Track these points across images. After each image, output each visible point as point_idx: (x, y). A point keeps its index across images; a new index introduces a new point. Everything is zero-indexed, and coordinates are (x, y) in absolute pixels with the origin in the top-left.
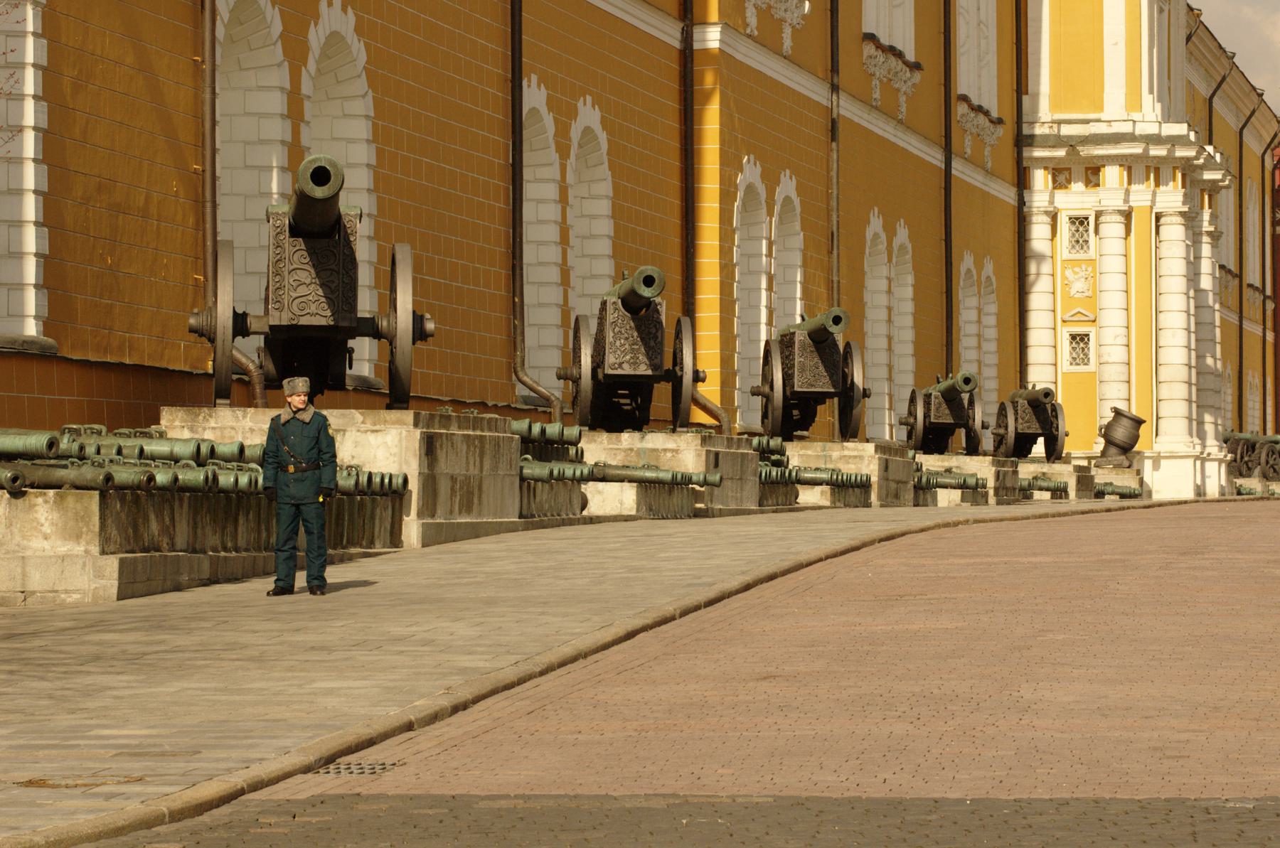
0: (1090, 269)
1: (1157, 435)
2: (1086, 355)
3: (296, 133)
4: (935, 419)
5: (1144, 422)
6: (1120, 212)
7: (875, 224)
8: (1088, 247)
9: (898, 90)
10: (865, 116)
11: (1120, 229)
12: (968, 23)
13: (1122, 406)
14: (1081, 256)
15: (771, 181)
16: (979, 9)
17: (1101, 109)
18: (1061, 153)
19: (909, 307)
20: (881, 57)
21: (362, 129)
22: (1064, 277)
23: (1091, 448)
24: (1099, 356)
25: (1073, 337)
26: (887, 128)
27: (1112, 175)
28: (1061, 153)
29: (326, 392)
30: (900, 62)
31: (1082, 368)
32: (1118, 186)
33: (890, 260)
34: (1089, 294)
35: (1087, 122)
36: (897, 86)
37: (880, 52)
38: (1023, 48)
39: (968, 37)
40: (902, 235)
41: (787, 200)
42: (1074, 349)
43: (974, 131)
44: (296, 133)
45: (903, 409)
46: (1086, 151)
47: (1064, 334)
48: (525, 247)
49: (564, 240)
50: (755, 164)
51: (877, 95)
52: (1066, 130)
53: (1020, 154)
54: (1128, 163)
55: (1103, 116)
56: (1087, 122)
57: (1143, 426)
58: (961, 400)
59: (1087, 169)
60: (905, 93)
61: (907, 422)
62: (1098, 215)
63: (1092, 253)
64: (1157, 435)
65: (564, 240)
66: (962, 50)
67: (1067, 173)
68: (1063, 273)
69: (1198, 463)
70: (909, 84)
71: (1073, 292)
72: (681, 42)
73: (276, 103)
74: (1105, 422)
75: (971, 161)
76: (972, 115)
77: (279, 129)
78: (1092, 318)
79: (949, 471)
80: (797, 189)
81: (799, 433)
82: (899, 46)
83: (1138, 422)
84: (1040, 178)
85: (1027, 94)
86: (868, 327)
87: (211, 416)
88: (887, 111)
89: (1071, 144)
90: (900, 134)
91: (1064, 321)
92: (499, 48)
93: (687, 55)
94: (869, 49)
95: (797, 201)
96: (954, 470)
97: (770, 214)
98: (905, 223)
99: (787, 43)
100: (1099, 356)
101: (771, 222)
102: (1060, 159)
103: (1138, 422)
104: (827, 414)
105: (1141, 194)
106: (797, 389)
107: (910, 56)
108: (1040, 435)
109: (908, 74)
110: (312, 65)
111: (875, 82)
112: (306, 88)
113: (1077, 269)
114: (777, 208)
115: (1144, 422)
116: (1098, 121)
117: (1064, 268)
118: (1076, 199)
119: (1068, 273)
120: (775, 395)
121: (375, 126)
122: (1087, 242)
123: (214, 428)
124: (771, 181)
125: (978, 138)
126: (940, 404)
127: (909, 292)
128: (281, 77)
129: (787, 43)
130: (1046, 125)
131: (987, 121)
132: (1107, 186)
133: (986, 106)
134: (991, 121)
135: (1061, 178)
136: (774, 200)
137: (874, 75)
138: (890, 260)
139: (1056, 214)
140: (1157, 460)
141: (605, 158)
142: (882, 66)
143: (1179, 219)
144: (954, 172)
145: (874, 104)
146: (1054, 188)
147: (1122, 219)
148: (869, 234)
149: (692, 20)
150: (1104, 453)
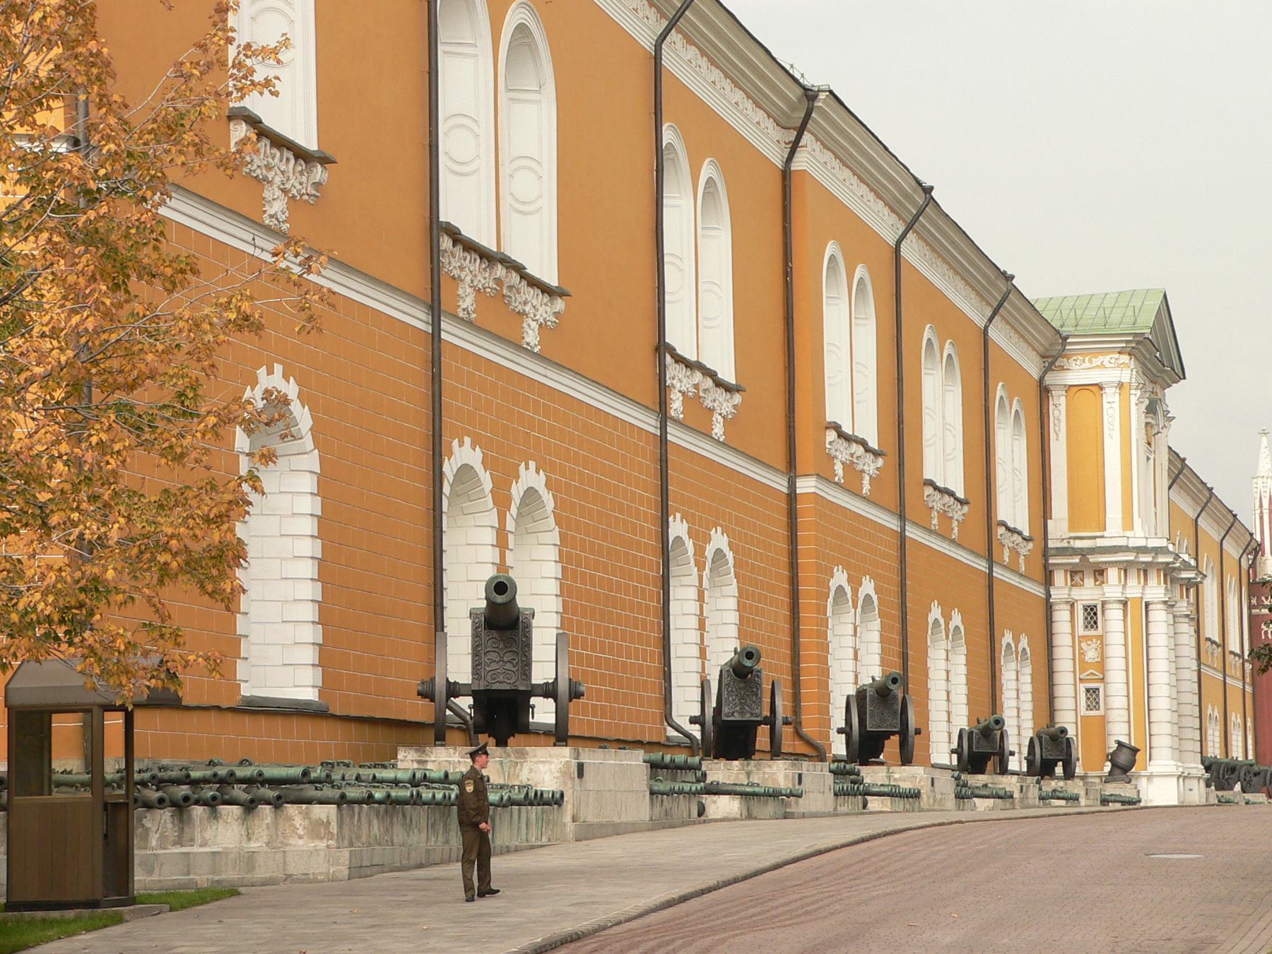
0: (1099, 642)
1: (1150, 759)
2: (1097, 703)
3: (502, 557)
4: (977, 748)
5: (1138, 750)
6: (1120, 602)
7: (936, 613)
8: (1097, 627)
9: (952, 518)
10: (927, 537)
11: (1119, 614)
12: (1005, 470)
13: (1125, 740)
14: (1092, 632)
15: (855, 583)
16: (1013, 460)
17: (1105, 530)
18: (1076, 560)
19: (963, 670)
20: (937, 495)
21: (553, 554)
22: (1081, 648)
23: (1103, 770)
24: (1105, 703)
25: (1088, 690)
26: (944, 545)
27: (1112, 574)
28: (1076, 560)
29: (516, 735)
30: (952, 499)
31: (1094, 713)
32: (1117, 583)
33: (947, 638)
34: (1099, 660)
35: (1095, 538)
36: (951, 515)
37: (937, 493)
38: (1048, 486)
39: (1005, 480)
40: (957, 619)
41: (868, 597)
42: (1088, 699)
43: (1011, 545)
44: (502, 557)
45: (955, 745)
46: (1093, 559)
47: (1082, 688)
48: (672, 632)
49: (702, 626)
50: (843, 572)
51: (935, 521)
52: (1078, 544)
53: (1046, 561)
54: (1125, 568)
55: (1106, 534)
56: (1095, 538)
57: (1138, 754)
58: (996, 735)
59: (1095, 571)
60: (957, 520)
61: (957, 751)
62: (1104, 603)
63: (1100, 631)
64: (1150, 759)
65: (702, 626)
66: (1001, 489)
67: (1081, 575)
68: (1079, 645)
69: (1181, 780)
70: (960, 513)
71: (1087, 659)
72: (788, 488)
73: (489, 536)
74: (1111, 751)
75: (1005, 567)
76: (1010, 534)
77: (491, 555)
78: (1101, 676)
79: (985, 786)
80: (875, 589)
81: (873, 759)
82: (952, 488)
83: (1135, 751)
84: (1059, 578)
85: (1051, 518)
86: (931, 684)
87: (432, 753)
88: (944, 536)
89: (1083, 553)
90: (953, 549)
91: (1080, 679)
92: (653, 497)
93: (792, 497)
94: (929, 490)
95: (875, 598)
96: (989, 785)
97: (855, 607)
98: (958, 611)
99: (866, 488)
100: (1105, 703)
101: (855, 613)
102: (1076, 564)
103: (1135, 751)
104: (892, 745)
105: (1134, 589)
106: (868, 729)
107: (961, 495)
108: (1060, 760)
109: (959, 506)
110: (514, 510)
111: (935, 514)
112: (510, 525)
113: (1089, 642)
114: (860, 602)
115: (1138, 750)
116: (1103, 537)
117: (1080, 642)
118: (1087, 593)
119: (1083, 645)
120: (854, 733)
121: (560, 551)
122: (1095, 623)
123: (434, 761)
124: (855, 583)
125: (1015, 553)
126: (979, 738)
127: (962, 659)
128: (493, 518)
129: (866, 488)
130: (1065, 541)
131: (1020, 538)
132: (1110, 583)
133: (1019, 528)
134: (1024, 539)
135: (1077, 578)
136: (857, 597)
137: (933, 508)
138: (947, 638)
139: (1073, 603)
140: (1150, 777)
141: (732, 570)
142: (937, 501)
143: (1162, 606)
144: (994, 574)
145: (933, 528)
146: (1072, 585)
147: (1121, 606)
148: (931, 620)
149: (795, 473)
150: (1110, 773)
